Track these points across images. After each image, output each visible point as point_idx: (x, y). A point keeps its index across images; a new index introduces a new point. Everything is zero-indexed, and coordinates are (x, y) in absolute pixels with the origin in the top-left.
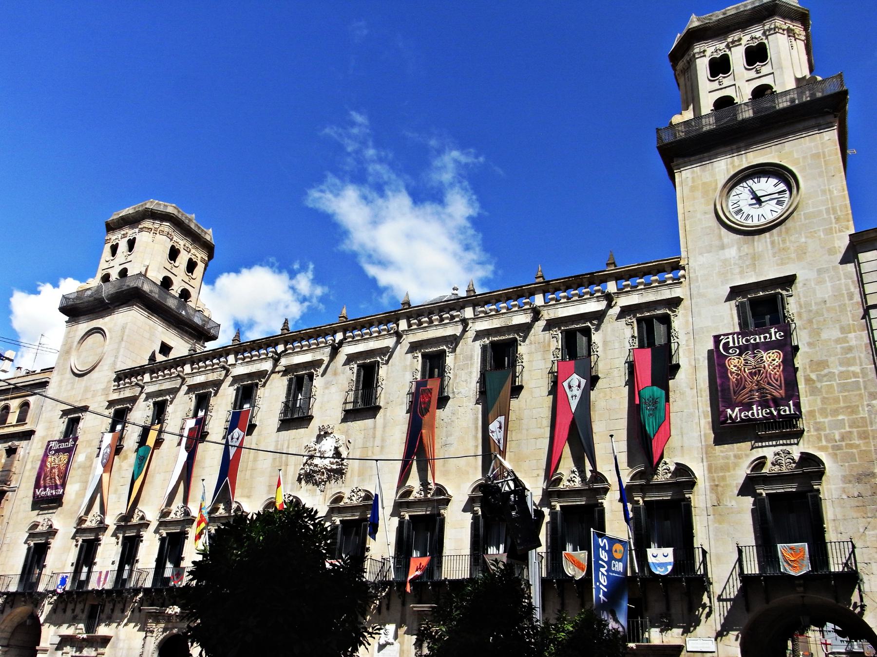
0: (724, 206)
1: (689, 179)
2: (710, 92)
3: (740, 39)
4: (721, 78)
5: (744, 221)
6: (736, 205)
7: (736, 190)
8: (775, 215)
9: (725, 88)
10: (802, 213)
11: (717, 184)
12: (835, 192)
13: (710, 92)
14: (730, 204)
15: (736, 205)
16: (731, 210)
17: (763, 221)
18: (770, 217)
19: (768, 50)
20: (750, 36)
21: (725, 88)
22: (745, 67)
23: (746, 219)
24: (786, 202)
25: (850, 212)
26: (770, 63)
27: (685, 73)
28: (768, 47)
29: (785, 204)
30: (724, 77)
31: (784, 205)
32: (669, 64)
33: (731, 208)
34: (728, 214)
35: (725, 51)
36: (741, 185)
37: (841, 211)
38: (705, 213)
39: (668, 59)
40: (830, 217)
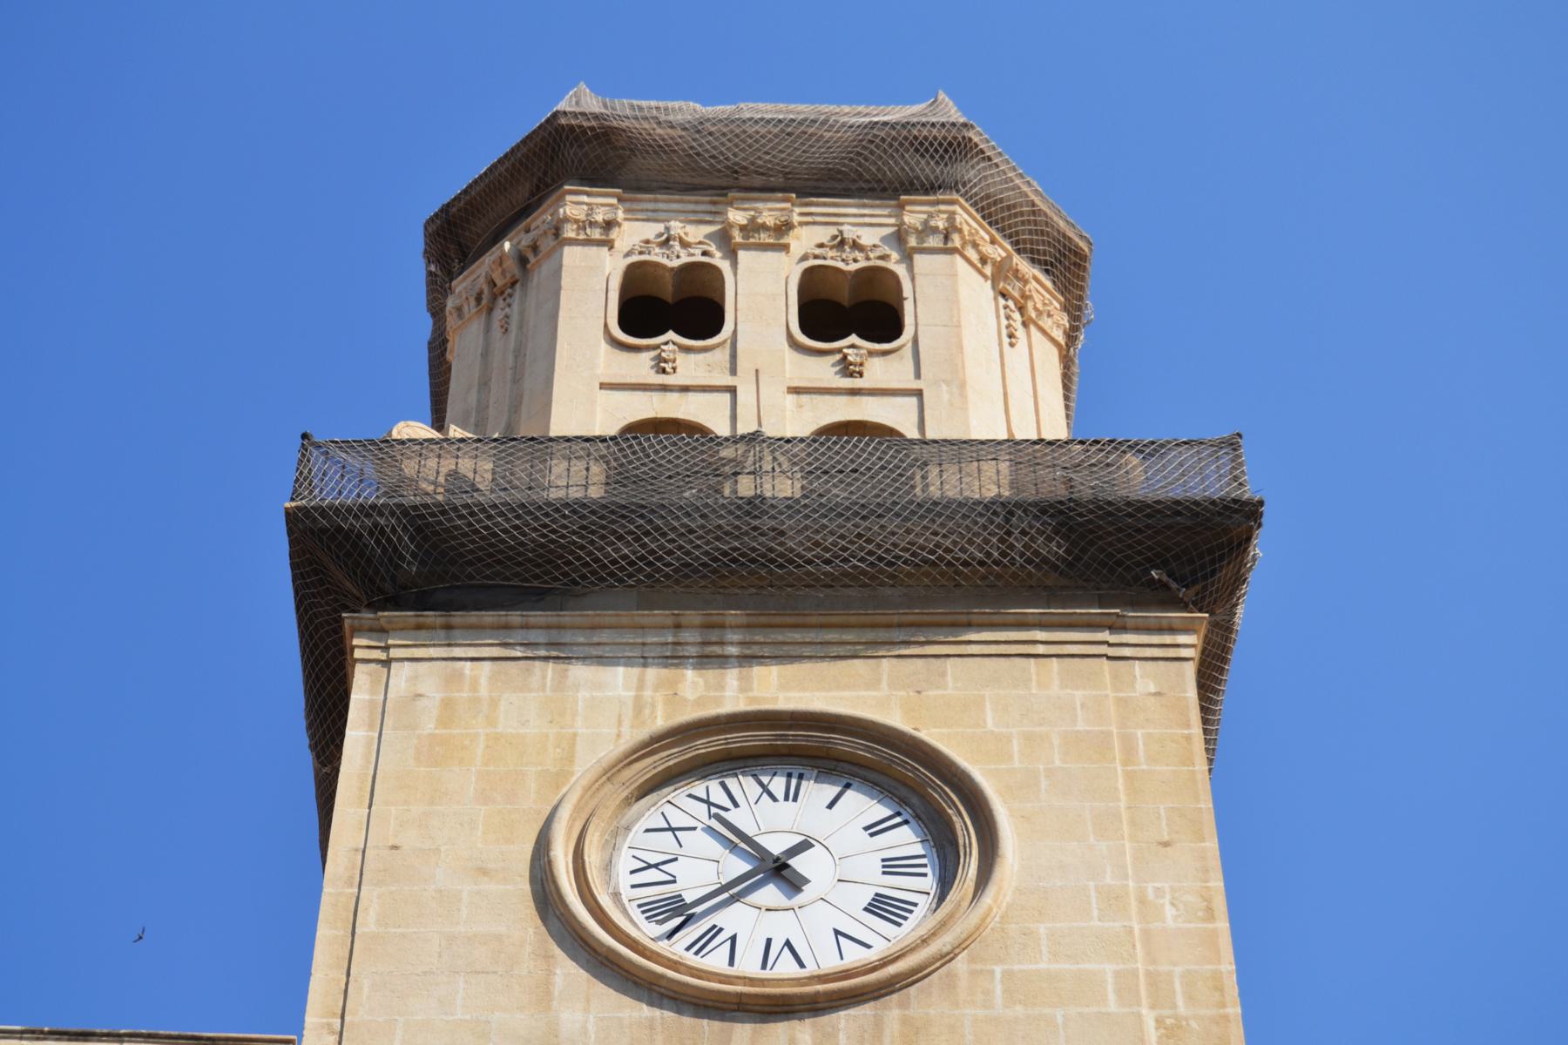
0: (592, 858)
1: (422, 703)
2: (603, 386)
3: (785, 228)
4: (671, 347)
5: (691, 959)
6: (653, 875)
7: (668, 809)
8: (855, 956)
9: (685, 389)
10: (998, 970)
11: (570, 758)
12: (1169, 912)
13: (603, 386)
14: (625, 862)
15: (653, 875)
16: (626, 893)
17: (786, 967)
18: (824, 958)
19: (908, 307)
20: (833, 231)
21: (685, 389)
22: (790, 336)
23: (700, 945)
24: (919, 912)
25: (1235, 1010)
26: (908, 351)
27: (490, 310)
28: (907, 291)
29: (914, 919)
30: (687, 350)
31: (907, 926)
32: (415, 269)
33: (624, 881)
34: (605, 901)
35: (705, 253)
36: (699, 789)
37: (1190, 998)
38: (484, 872)
39: (418, 242)
40: (1139, 1016)
